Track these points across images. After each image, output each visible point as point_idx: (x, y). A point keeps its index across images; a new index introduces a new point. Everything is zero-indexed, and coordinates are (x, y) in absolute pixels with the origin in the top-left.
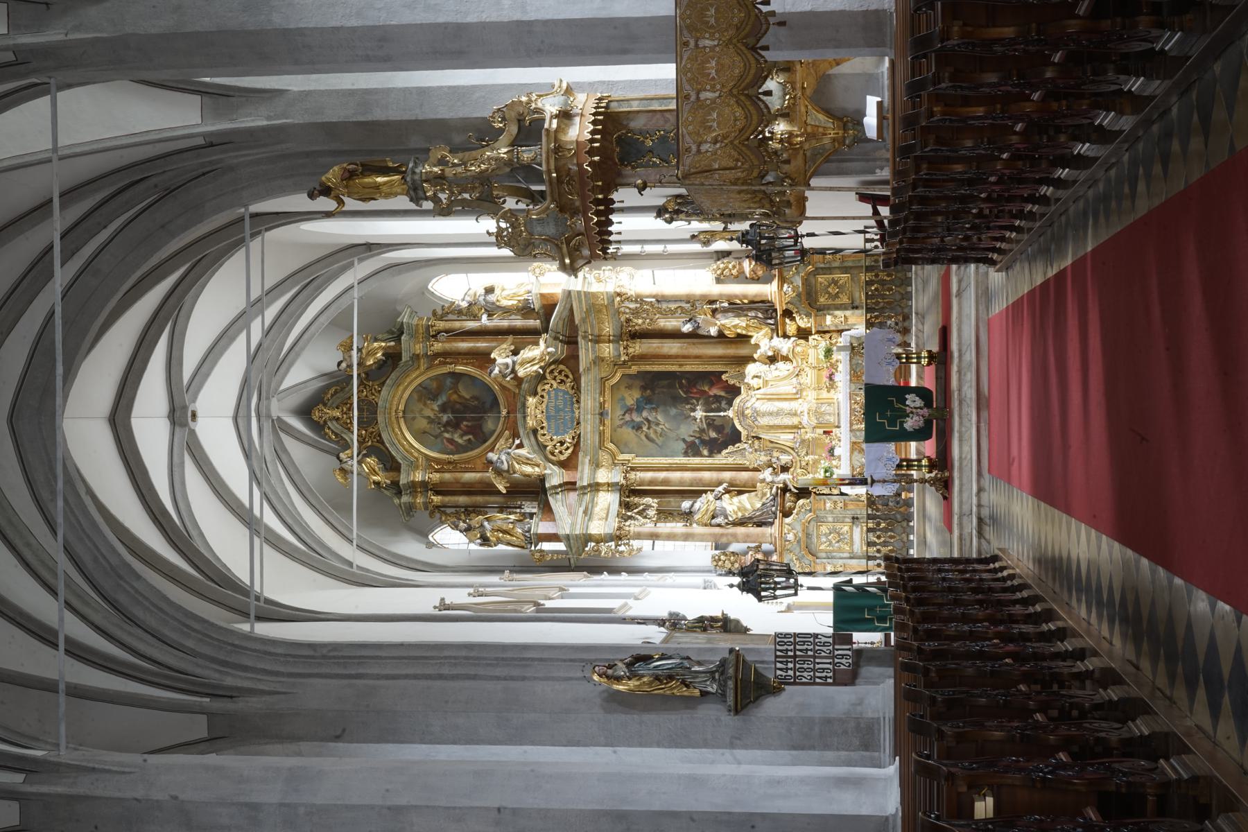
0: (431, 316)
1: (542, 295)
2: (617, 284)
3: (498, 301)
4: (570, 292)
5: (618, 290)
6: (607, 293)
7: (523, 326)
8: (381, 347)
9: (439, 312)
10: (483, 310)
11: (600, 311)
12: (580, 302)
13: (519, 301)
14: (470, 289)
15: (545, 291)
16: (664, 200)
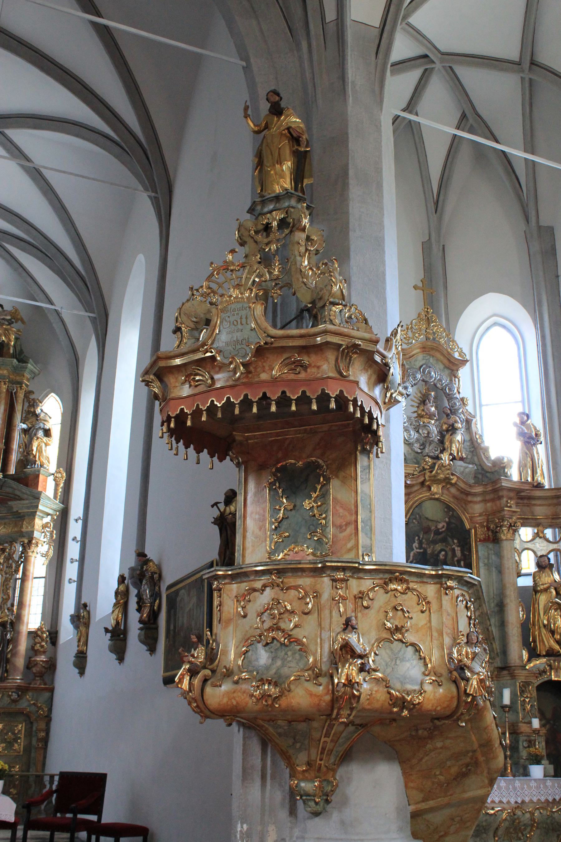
0: (30, 389)
1: (38, 476)
2: (40, 542)
3: (38, 438)
4: (38, 499)
5: (34, 541)
6: (33, 532)
7: (11, 460)
8: (10, 340)
9: (32, 397)
10: (30, 426)
11: (16, 525)
12: (28, 508)
13: (35, 457)
14: (50, 418)
15: (41, 478)
16: (156, 563)
